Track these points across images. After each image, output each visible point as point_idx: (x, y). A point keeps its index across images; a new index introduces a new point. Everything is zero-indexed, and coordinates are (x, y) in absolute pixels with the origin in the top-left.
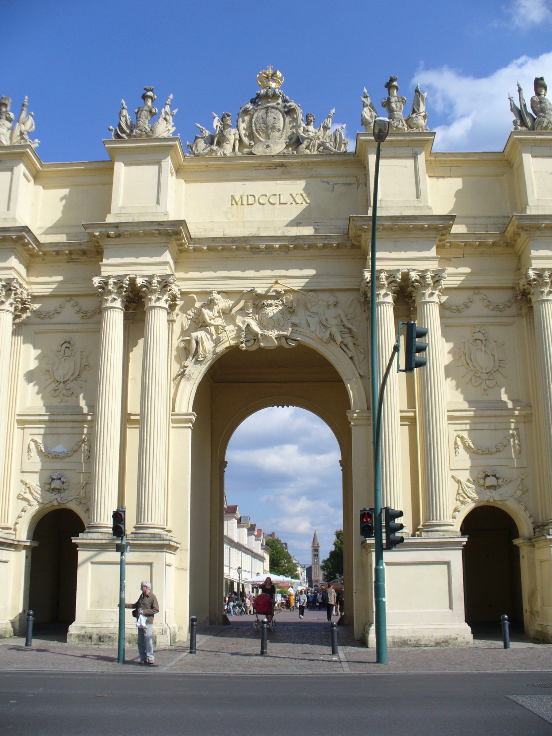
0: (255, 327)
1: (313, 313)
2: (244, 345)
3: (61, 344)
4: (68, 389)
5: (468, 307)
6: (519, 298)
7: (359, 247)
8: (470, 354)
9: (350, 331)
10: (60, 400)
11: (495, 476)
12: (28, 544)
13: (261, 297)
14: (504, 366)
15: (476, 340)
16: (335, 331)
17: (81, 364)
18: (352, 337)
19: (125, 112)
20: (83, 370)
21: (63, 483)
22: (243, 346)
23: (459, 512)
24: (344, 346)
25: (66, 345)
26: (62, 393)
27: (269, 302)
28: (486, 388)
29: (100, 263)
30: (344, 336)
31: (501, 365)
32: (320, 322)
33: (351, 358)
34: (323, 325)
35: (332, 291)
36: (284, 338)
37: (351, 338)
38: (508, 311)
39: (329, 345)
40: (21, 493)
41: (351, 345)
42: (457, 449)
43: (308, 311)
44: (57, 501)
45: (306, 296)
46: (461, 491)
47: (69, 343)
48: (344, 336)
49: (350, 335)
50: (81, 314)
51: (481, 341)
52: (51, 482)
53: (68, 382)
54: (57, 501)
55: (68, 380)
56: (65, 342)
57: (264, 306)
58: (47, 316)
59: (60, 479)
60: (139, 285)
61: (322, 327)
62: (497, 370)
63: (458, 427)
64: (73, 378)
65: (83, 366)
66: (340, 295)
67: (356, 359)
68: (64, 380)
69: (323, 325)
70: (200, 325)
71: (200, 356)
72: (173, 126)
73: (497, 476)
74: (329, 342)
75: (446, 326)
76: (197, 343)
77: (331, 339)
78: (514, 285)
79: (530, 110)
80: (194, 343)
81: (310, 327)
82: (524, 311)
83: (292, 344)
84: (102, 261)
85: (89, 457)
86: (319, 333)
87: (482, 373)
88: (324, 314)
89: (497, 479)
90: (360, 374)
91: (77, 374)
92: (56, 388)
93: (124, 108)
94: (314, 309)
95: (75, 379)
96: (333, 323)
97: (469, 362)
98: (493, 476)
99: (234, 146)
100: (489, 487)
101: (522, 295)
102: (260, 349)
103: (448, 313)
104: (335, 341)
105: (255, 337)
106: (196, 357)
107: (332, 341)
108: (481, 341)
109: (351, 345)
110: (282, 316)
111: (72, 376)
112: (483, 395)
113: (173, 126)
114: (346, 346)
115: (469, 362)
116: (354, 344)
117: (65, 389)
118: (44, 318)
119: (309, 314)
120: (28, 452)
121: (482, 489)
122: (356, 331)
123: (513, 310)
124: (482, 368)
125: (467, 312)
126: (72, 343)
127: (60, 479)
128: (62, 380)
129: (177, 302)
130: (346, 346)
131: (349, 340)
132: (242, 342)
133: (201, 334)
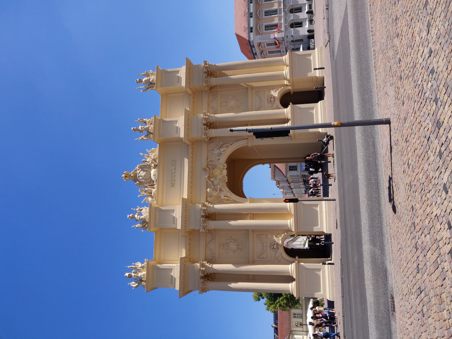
8: (230, 107)
9: (222, 145)
11: (270, 98)
16: (222, 150)
17: (231, 240)
18: (224, 145)
19: (137, 226)
33: (231, 145)
35: (208, 152)
41: (227, 145)
50: (213, 240)
56: (223, 246)
67: (231, 144)
70: (218, 196)
72: (144, 207)
76: (224, 196)
83: (225, 164)
90: (237, 142)
91: (235, 241)
93: (135, 226)
97: (232, 107)
100: (274, 100)
109: (227, 145)
113: (144, 207)
114: (227, 147)
115: (232, 107)
116: (226, 144)
126: (223, 244)
128: (237, 246)
130: (227, 147)
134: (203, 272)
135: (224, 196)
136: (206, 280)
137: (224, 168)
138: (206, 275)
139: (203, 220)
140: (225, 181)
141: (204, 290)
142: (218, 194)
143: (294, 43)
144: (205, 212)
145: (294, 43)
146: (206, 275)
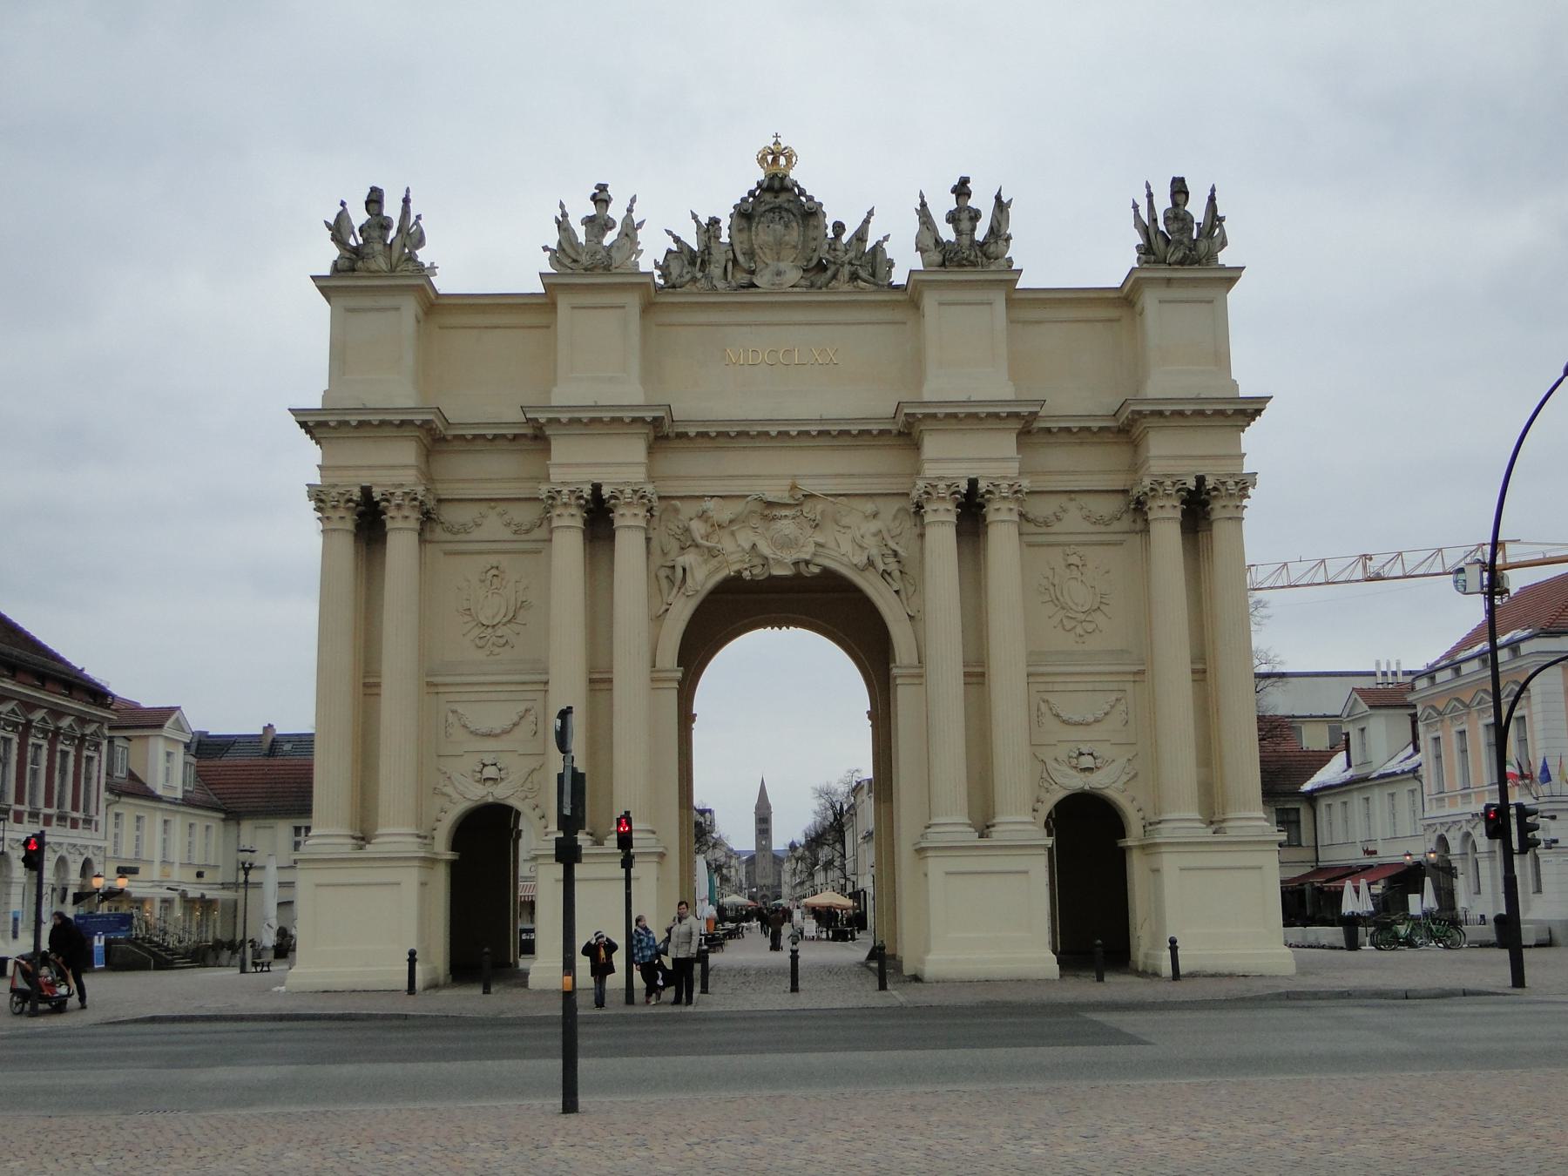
0: (765, 549)
1: (844, 527)
2: (748, 572)
3: (485, 570)
4: (500, 637)
5: (1059, 519)
6: (1132, 506)
7: (909, 434)
9: (895, 554)
10: (488, 653)
11: (1091, 754)
12: (449, 857)
13: (770, 504)
14: (1107, 602)
15: (1070, 565)
18: (899, 562)
20: (520, 608)
21: (500, 770)
22: (746, 575)
23: (1042, 802)
24: (885, 574)
25: (494, 572)
26: (490, 642)
27: (784, 512)
28: (1082, 633)
29: (548, 462)
30: (887, 560)
31: (1103, 600)
32: (854, 540)
33: (897, 592)
34: (857, 544)
36: (804, 564)
37: (897, 563)
38: (1116, 526)
39: (867, 573)
40: (438, 787)
41: (896, 574)
42: (1041, 718)
43: (837, 524)
44: (493, 795)
45: (834, 504)
46: (1045, 775)
47: (497, 568)
48: (887, 560)
49: (896, 560)
51: (1078, 566)
52: (482, 770)
53: (500, 625)
54: (493, 795)
55: (499, 622)
57: (774, 518)
58: (463, 530)
59: (495, 764)
60: (607, 496)
61: (857, 547)
62: (1099, 608)
63: (1042, 687)
64: (505, 619)
65: (519, 603)
66: (880, 502)
67: (903, 594)
68: (494, 623)
69: (857, 544)
71: (689, 589)
73: (1095, 754)
74: (867, 569)
75: (1030, 545)
76: (684, 570)
77: (870, 565)
78: (1126, 488)
79: (1162, 227)
80: (679, 572)
81: (839, 547)
82: (1139, 525)
83: (816, 570)
84: (550, 459)
85: (535, 733)
86: (853, 555)
87: (1077, 612)
88: (859, 529)
89: (1095, 758)
92: (482, 635)
94: (845, 521)
95: (510, 621)
96: (871, 543)
98: (1089, 754)
99: (726, 267)
101: (1136, 503)
102: (771, 578)
103: (1031, 528)
104: (875, 568)
105: (765, 561)
106: (682, 590)
107: (870, 568)
108: (1078, 566)
110: (801, 531)
111: (504, 617)
112: (1077, 642)
116: (901, 572)
117: (497, 637)
118: (458, 533)
119: (838, 528)
120: (446, 727)
121: (1073, 772)
122: (903, 554)
123: (1125, 523)
124: (1077, 604)
125: (1057, 527)
127: (495, 764)
129: (654, 513)
131: (893, 566)
132: (746, 569)
133: (689, 558)
134: (389, 496)
135: (684, 570)
136: (360, 508)
137: (802, 566)
138: (380, 508)
139: (581, 491)
140: (746, 569)
141: (319, 497)
142: (694, 543)
143: (1498, 853)
144: (616, 498)
145: (1498, 853)
146: (380, 508)
